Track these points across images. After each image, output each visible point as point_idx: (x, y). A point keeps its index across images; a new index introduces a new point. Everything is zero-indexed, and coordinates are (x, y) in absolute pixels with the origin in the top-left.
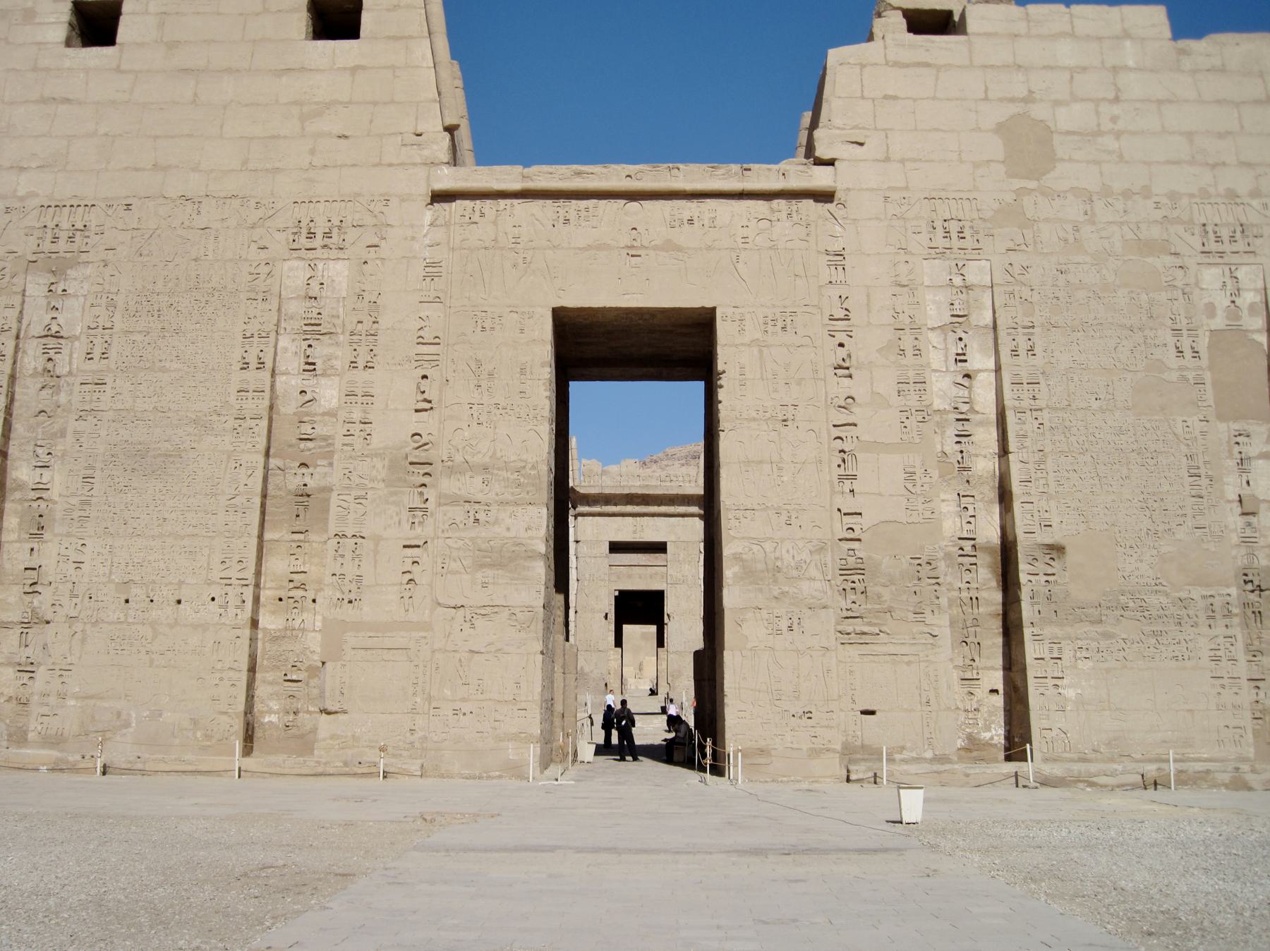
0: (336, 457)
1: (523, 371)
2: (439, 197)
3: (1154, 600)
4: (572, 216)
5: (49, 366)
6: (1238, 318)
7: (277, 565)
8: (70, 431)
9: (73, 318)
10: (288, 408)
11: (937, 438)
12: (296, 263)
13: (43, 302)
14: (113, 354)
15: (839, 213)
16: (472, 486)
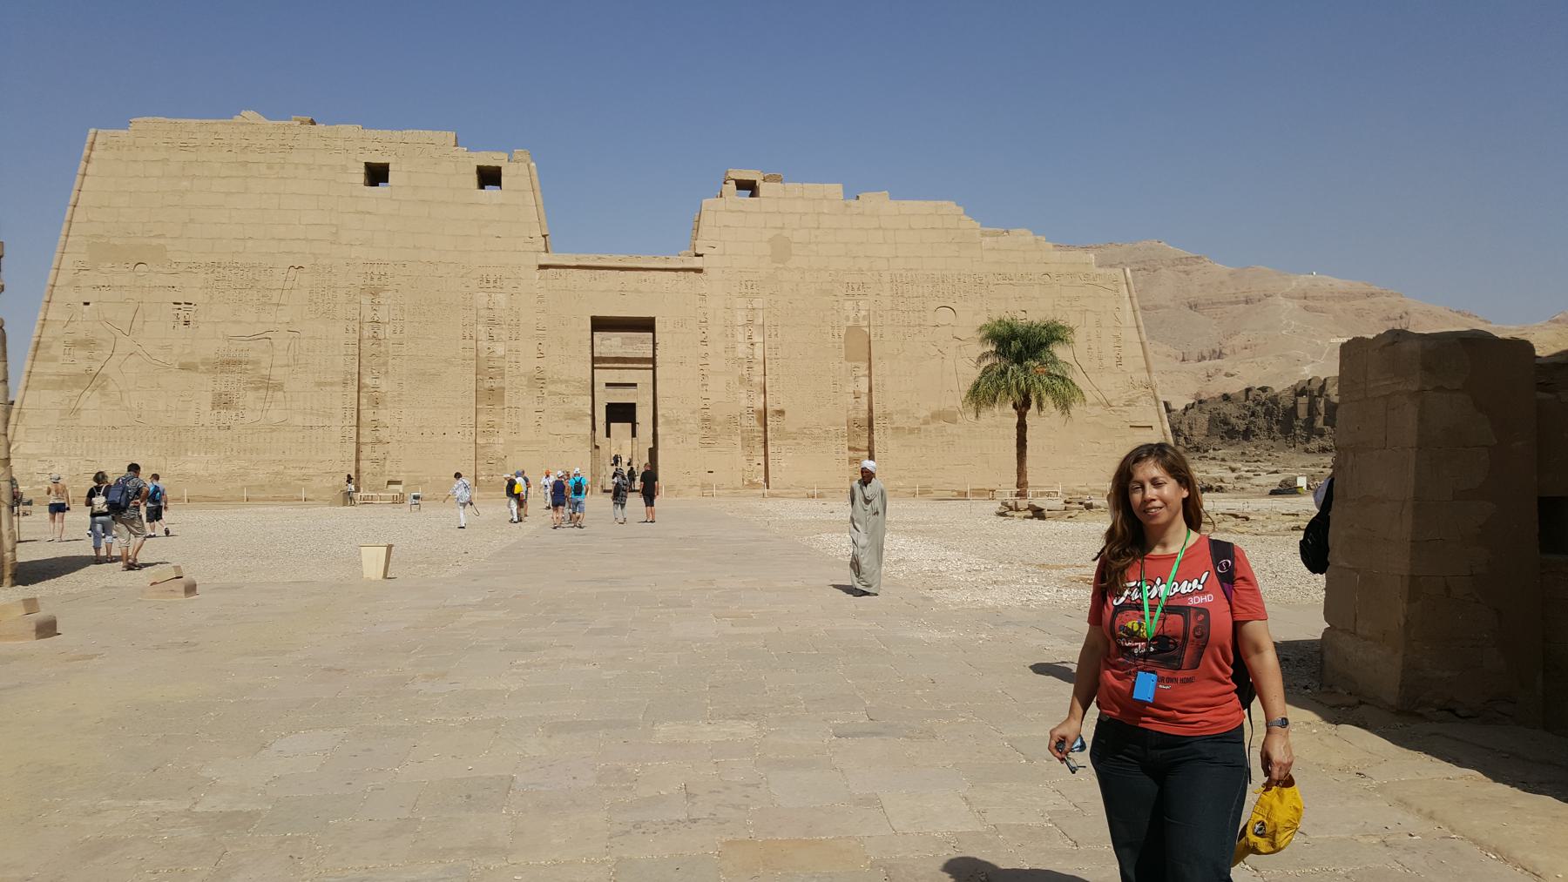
0: (506, 376)
1: (580, 342)
2: (542, 267)
3: (816, 431)
4: (597, 277)
5: (375, 335)
6: (858, 321)
7: (483, 418)
8: (390, 364)
9: (382, 315)
10: (483, 355)
11: (739, 369)
12: (481, 294)
13: (370, 307)
14: (405, 331)
15: (705, 278)
16: (562, 388)
